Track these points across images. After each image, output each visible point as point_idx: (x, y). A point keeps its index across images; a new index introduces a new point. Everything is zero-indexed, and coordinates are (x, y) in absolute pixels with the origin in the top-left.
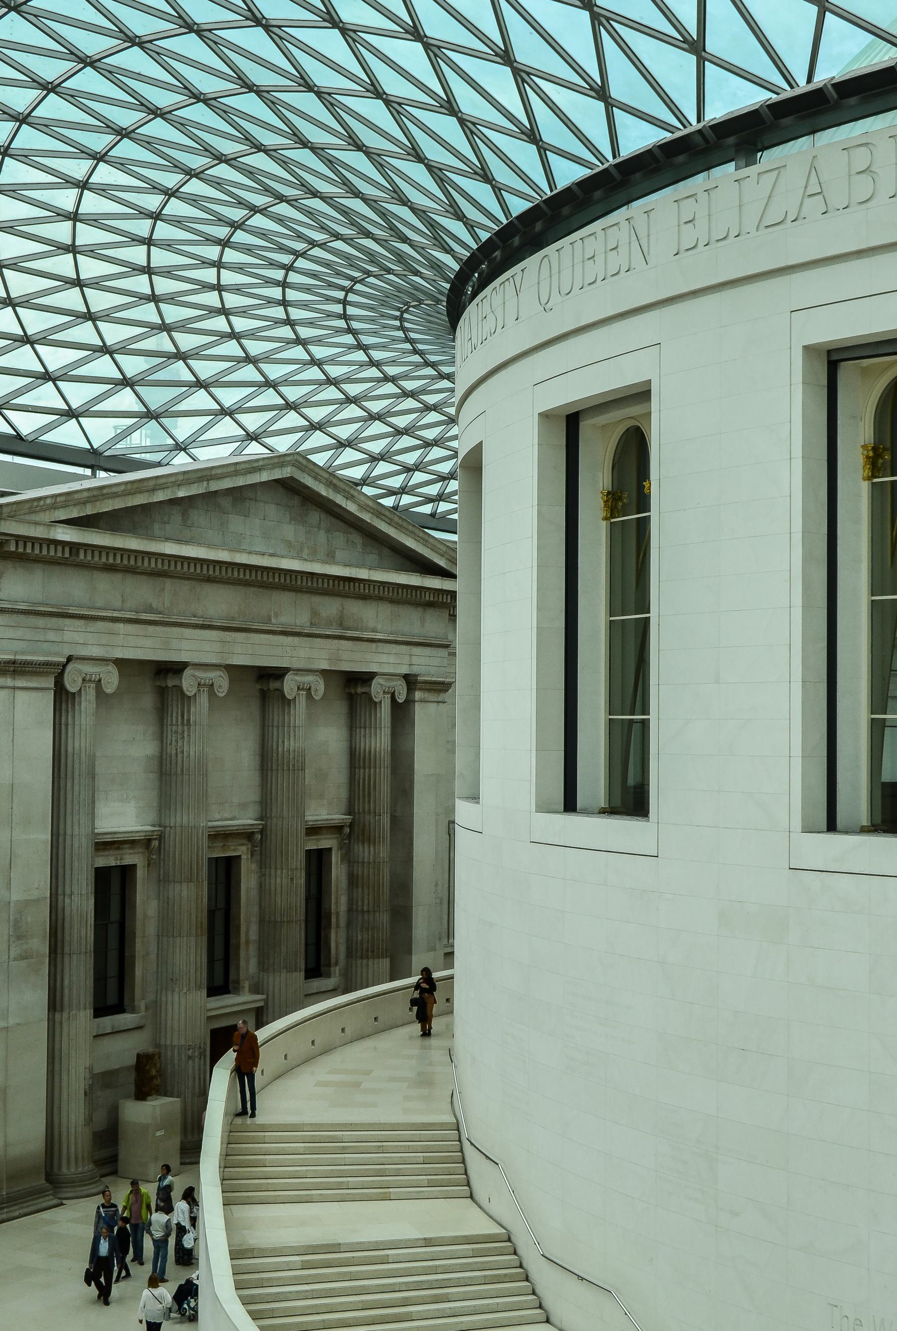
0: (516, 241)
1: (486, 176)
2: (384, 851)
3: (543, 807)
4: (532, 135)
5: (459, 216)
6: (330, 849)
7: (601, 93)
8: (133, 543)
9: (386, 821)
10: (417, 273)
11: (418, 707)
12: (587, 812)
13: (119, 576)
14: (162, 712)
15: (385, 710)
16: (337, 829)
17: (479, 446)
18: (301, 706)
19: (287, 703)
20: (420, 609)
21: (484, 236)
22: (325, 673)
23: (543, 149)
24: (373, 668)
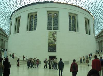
15: (4, 42)
22: (1, 39)
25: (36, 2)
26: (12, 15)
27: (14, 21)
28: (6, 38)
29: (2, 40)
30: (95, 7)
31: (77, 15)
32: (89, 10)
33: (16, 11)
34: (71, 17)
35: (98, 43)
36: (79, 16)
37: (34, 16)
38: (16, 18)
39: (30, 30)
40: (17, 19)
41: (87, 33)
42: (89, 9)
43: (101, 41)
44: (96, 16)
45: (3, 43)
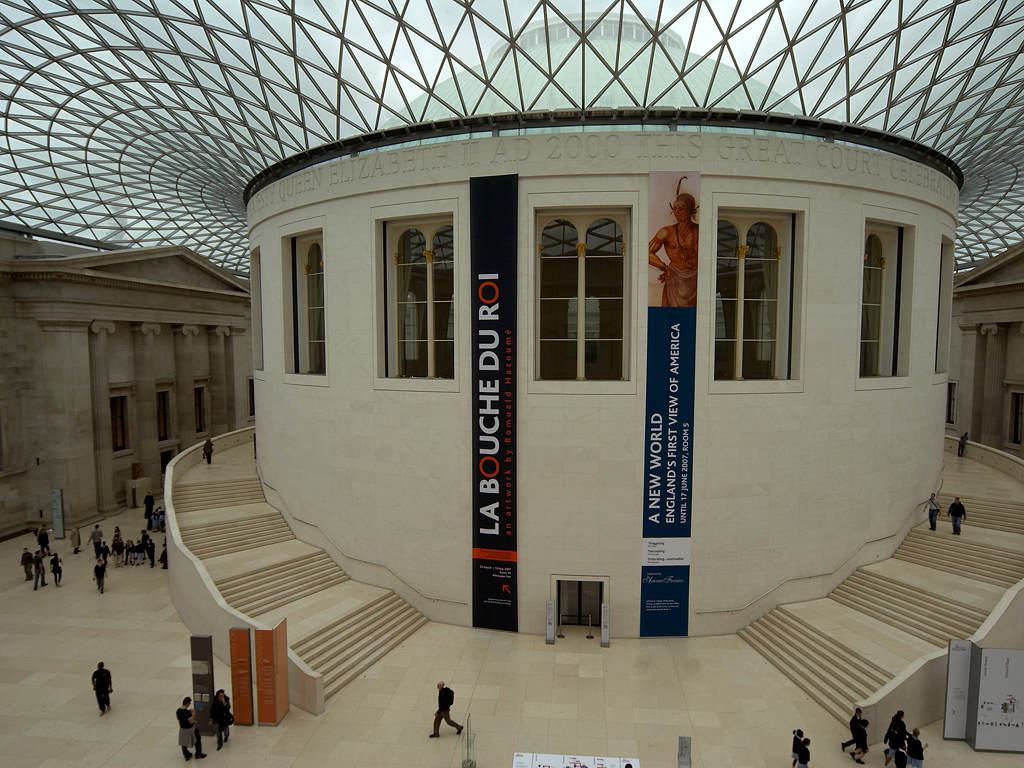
0: (270, 175)
1: (258, 150)
3: (287, 372)
4: (276, 137)
5: (248, 164)
6: (203, 388)
7: (302, 125)
10: (231, 183)
12: (303, 374)
15: (222, 338)
16: (206, 380)
17: (259, 247)
18: (189, 338)
21: (258, 172)
22: (199, 326)
23: (280, 143)
29: (209, 330)
34: (743, 240)
35: (973, 336)
36: (812, 234)
41: (867, 368)
43: (1006, 328)
45: (220, 349)
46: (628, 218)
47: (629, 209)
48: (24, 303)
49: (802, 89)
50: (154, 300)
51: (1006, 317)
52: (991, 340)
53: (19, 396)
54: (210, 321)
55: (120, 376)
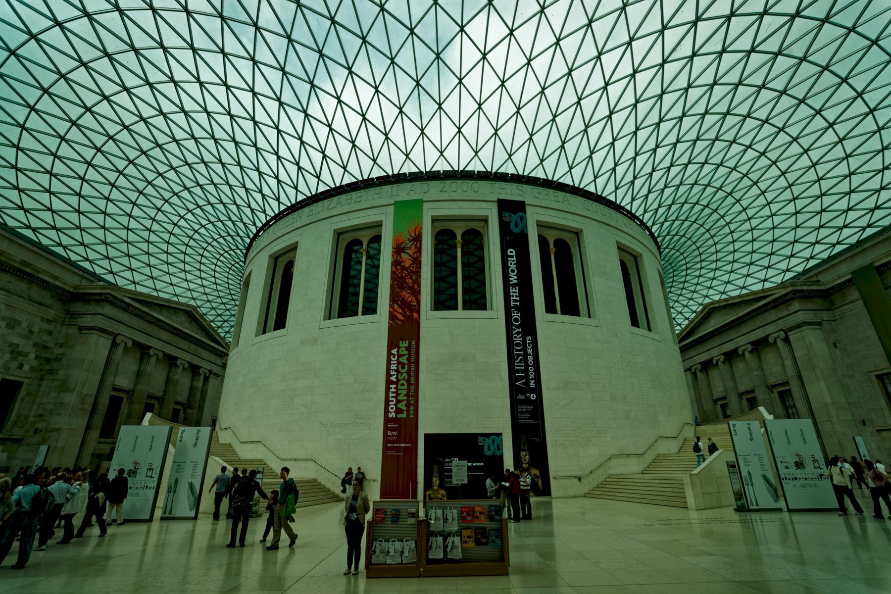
2: (195, 412)
8: (146, 309)
9: (197, 404)
11: (211, 379)
13: (138, 319)
14: (141, 359)
15: (202, 378)
19: (177, 366)
20: (215, 356)
22: (189, 363)
24: (201, 365)
25: (374, 175)
26: (252, 240)
27: (259, 268)
28: (219, 361)
29: (194, 369)
30: (663, 190)
31: (578, 234)
32: (636, 208)
33: (272, 218)
34: (552, 246)
36: (589, 240)
37: (365, 247)
38: (271, 256)
39: (342, 314)
40: (275, 259)
41: (635, 322)
42: (636, 204)
44: (668, 238)
45: (199, 384)
46: (486, 226)
47: (485, 220)
48: (74, 315)
49: (572, 170)
50: (165, 335)
51: (704, 357)
52: (698, 373)
53: (42, 379)
54: (197, 361)
55: (124, 382)
